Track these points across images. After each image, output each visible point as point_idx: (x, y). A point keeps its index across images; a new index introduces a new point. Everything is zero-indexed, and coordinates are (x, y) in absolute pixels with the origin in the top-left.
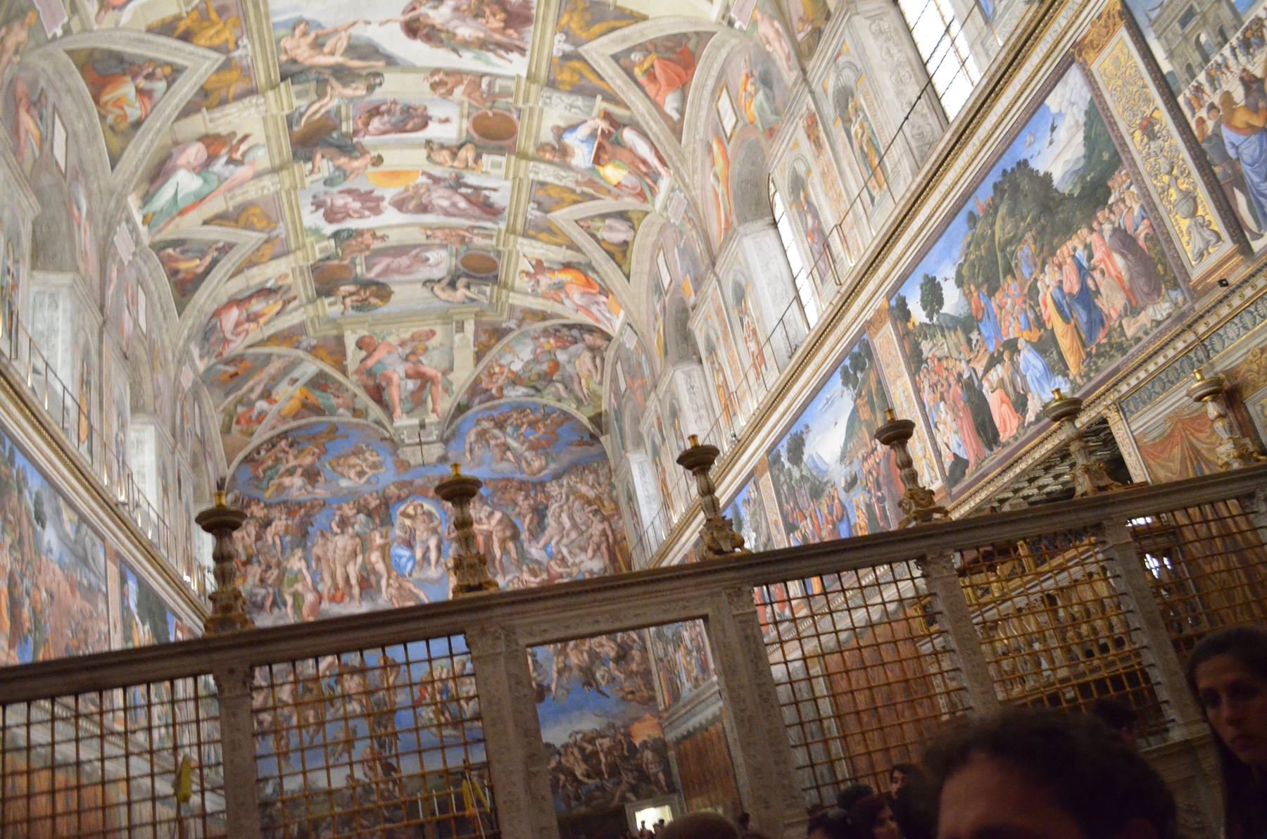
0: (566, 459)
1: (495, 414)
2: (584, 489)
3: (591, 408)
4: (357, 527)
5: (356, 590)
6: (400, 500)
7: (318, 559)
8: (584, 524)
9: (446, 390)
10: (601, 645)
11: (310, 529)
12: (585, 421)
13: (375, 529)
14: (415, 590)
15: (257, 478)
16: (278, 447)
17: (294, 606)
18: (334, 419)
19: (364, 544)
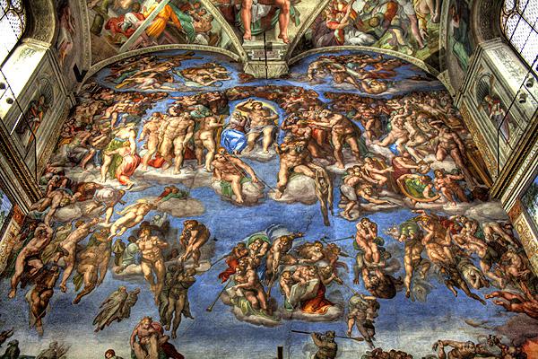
0: (405, 87)
1: (337, 56)
2: (426, 108)
3: (427, 50)
4: (192, 113)
5: (178, 160)
6: (240, 98)
7: (148, 132)
8: (429, 132)
9: (293, 19)
10: (465, 242)
11: (148, 111)
12: (420, 63)
13: (210, 116)
14: (243, 166)
15: (115, 77)
16: (141, 60)
17: (109, 165)
18: (193, 47)
19: (197, 125)
